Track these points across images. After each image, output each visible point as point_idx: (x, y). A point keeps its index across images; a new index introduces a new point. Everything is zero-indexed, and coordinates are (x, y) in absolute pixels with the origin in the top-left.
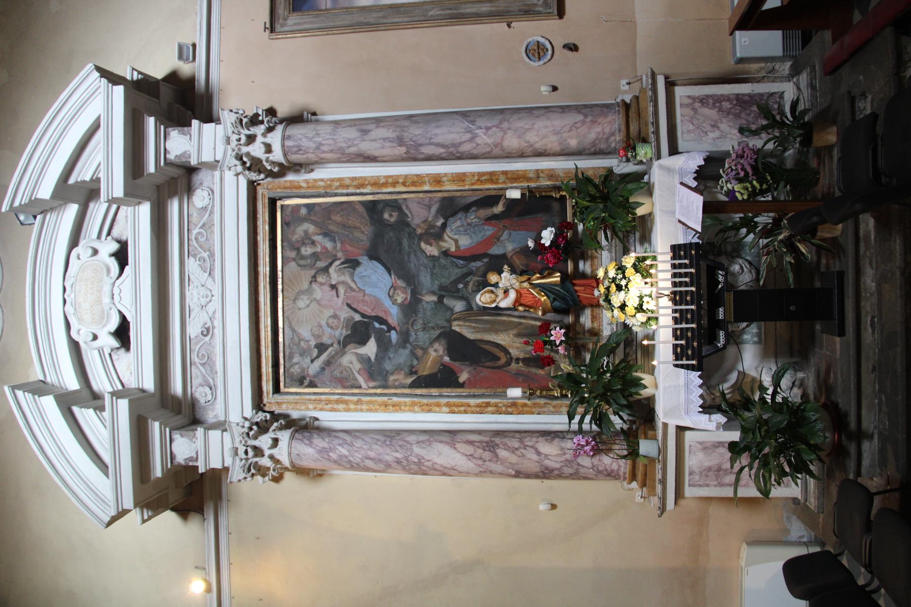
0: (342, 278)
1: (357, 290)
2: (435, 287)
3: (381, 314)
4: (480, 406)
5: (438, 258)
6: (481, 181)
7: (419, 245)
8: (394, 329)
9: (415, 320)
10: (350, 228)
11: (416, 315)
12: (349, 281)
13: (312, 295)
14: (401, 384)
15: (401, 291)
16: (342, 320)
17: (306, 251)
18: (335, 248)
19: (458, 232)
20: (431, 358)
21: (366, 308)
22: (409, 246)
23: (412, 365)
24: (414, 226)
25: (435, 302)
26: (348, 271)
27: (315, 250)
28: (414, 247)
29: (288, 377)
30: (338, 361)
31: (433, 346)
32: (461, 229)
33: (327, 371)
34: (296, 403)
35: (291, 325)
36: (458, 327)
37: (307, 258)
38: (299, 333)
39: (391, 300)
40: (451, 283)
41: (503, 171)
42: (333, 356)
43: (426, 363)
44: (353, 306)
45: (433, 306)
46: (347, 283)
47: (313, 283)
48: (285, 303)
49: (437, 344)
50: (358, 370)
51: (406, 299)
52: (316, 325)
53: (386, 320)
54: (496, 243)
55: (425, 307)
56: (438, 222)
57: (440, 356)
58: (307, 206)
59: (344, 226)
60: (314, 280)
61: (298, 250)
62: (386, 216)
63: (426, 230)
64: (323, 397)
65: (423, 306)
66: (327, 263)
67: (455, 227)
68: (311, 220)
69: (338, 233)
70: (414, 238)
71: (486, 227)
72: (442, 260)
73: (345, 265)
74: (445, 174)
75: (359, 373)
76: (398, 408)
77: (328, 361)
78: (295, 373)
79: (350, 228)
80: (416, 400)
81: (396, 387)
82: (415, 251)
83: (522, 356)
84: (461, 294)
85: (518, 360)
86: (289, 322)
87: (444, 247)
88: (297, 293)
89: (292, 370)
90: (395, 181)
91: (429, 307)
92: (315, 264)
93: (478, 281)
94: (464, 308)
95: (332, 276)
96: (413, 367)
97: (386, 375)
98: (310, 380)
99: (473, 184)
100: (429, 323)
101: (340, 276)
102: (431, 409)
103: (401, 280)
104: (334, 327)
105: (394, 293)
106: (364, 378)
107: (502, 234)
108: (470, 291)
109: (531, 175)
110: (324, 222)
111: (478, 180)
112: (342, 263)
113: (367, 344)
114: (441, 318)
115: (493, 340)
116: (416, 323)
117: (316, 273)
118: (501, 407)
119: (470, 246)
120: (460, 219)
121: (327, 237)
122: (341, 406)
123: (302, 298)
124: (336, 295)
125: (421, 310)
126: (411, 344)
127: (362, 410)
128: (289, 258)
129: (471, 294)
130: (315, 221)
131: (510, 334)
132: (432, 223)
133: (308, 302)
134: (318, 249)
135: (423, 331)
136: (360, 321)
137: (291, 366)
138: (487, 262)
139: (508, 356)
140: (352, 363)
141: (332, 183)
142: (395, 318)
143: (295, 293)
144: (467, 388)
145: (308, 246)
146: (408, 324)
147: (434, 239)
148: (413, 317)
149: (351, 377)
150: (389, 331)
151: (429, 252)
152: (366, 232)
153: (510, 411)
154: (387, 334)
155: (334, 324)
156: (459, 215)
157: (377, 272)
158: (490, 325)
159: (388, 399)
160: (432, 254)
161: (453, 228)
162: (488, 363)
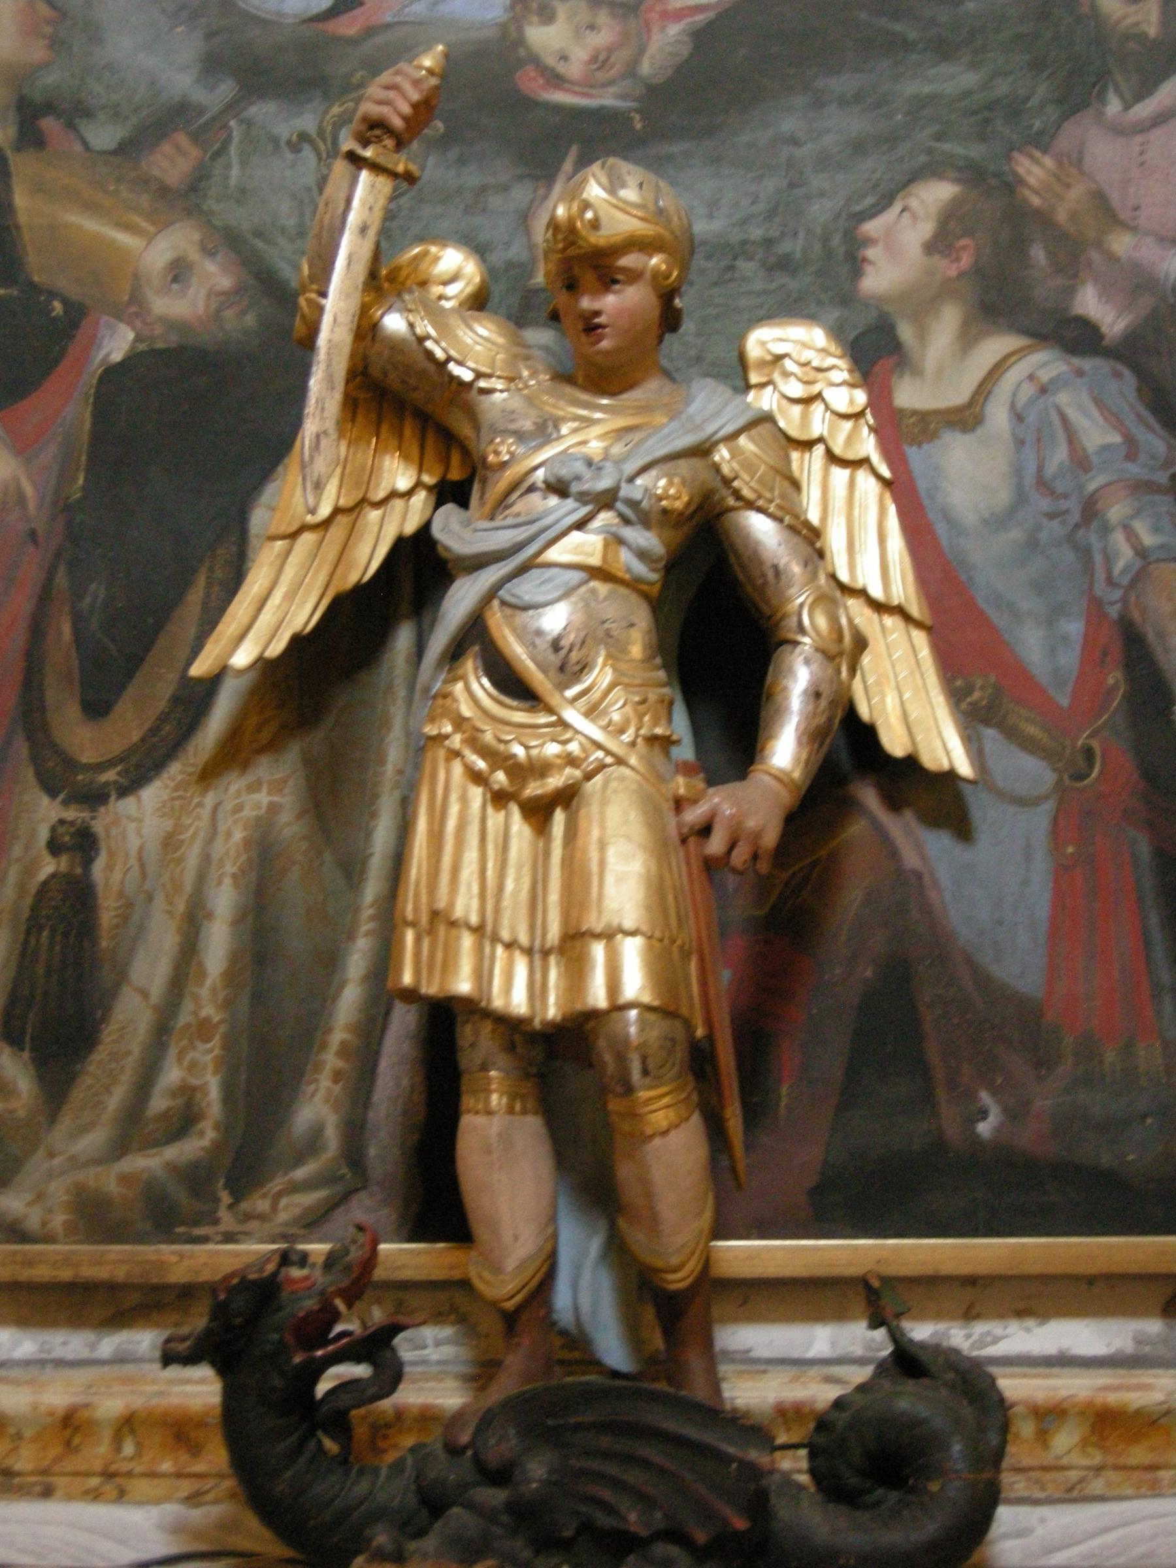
7: (930, 170)
15: (610, 50)
20: (124, 238)
22: (933, 98)
23: (88, 114)
24: (1068, 136)
31: (210, 253)
32: (1059, 455)
43: (90, 207)
51: (557, 80)
55: (495, 201)
56: (1107, 292)
57: (136, 298)
63: (1045, 219)
65: (505, 188)
67: (1073, 414)
70: (983, 138)
71: (1074, 628)
82: (891, 140)
87: (923, 335)
96: (71, 126)
103: (685, 51)
107: (1028, 745)
119: (932, 516)
120: (1131, 449)
125: (472, 178)
126: (231, 107)
132: (1095, 256)
139: (110, 776)
147: (977, 270)
151: (889, 232)
160: (871, 253)
161: (1063, 398)
162: (67, 629)
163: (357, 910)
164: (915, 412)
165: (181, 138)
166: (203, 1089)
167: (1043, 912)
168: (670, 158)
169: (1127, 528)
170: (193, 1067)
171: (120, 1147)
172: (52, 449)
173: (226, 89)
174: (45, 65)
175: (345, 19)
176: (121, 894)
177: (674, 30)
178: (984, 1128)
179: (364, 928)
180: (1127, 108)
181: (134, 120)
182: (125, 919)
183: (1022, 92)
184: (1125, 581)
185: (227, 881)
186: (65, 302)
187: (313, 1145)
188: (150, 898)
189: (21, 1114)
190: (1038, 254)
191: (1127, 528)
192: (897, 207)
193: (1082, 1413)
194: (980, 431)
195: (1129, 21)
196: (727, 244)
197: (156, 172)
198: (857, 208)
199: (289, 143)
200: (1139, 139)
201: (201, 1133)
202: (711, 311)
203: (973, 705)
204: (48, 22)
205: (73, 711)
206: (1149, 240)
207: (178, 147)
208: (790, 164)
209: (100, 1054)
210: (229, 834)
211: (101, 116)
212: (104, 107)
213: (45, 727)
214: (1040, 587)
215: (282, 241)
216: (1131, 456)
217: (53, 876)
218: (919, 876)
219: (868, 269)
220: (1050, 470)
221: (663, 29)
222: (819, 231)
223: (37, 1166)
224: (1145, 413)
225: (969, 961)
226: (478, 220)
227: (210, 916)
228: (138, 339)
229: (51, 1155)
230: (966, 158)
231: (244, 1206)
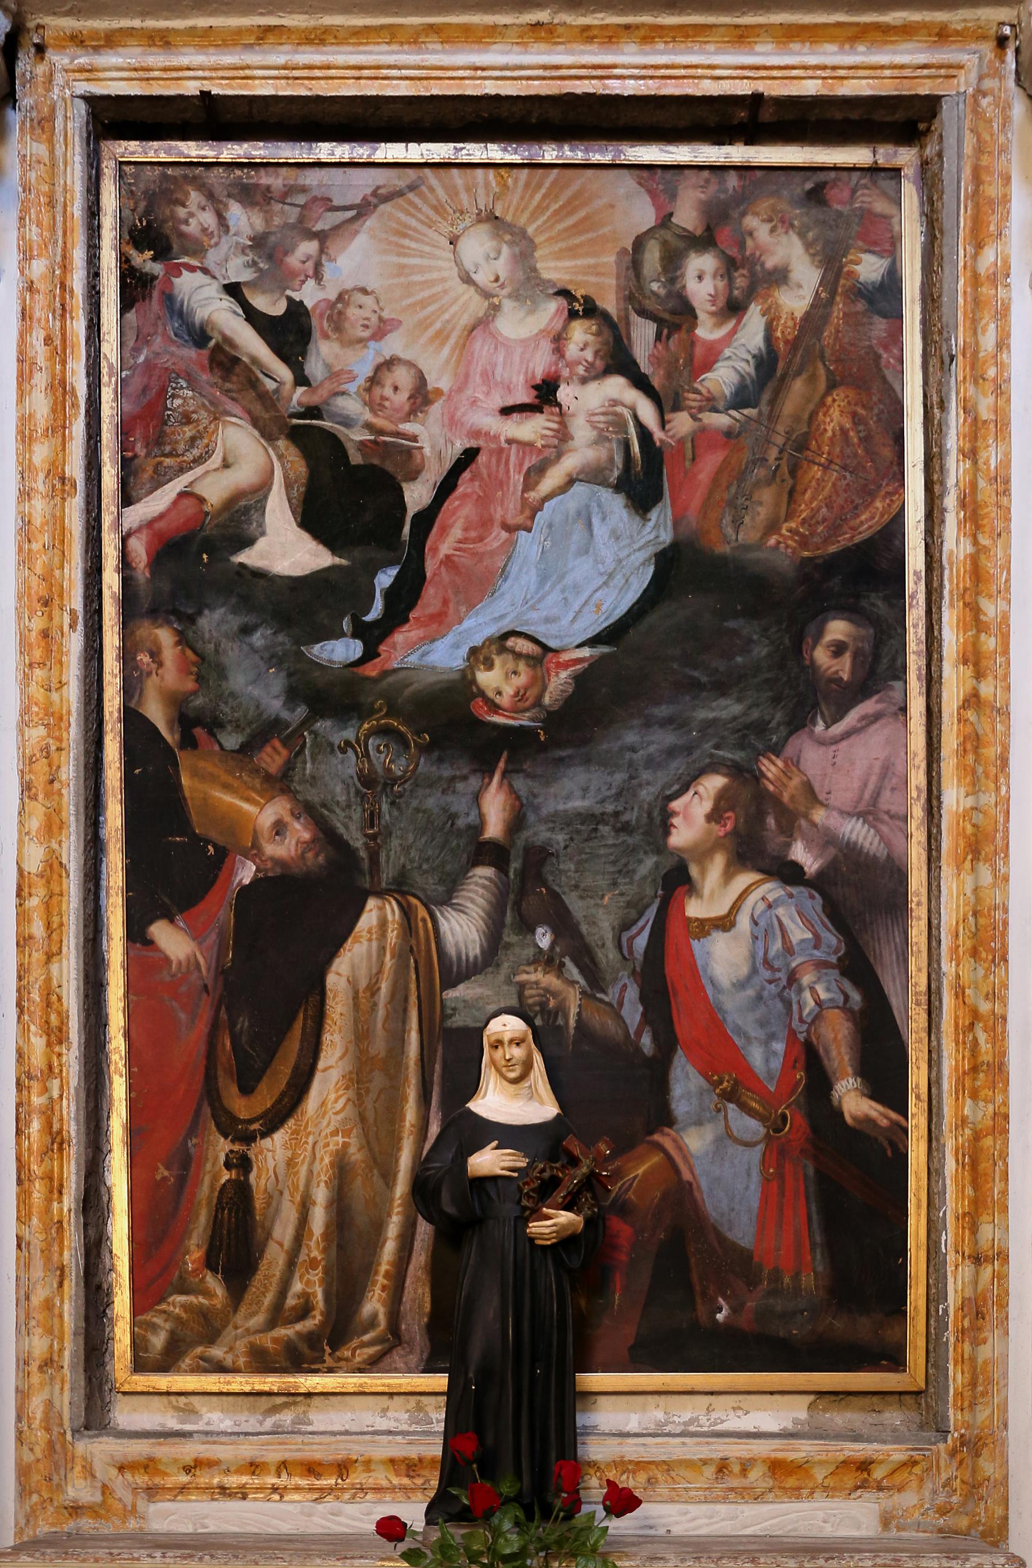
0: (582, 432)
1: (533, 496)
2: (539, 833)
3: (430, 598)
4: (48, 1005)
5: (660, 848)
6: (972, 1024)
8: (370, 654)
9: (406, 745)
10: (793, 472)
11: (425, 749)
12: (570, 463)
13: (515, 296)
14: (140, 680)
16: (407, 427)
17: (700, 278)
18: (711, 404)
19: (761, 932)
20: (246, 806)
21: (456, 532)
22: (714, 722)
23: (221, 726)
24: (789, 750)
25: (479, 827)
26: (611, 460)
27: (702, 316)
28: (707, 746)
29: (165, 177)
30: (230, 406)
31: (297, 818)
32: (777, 946)
33: (191, 353)
34: (51, 204)
35: (387, 198)
36: (374, 922)
37: (672, 281)
38: (357, 232)
39: (490, 640)
40: (556, 897)
41: (1006, 1117)
42: (253, 383)
43: (227, 787)
44: (466, 475)
45: (461, 823)
46: (559, 456)
47: (562, 302)
48: (479, 172)
49: (306, 836)
50: (198, 490)
52: (385, 315)
53: (406, 620)
54: (716, 1084)
55: (460, 786)
56: (808, 847)
57: (256, 845)
58: (891, 284)
59: (802, 445)
60: (577, 306)
61: (705, 241)
62: (838, 629)
63: (776, 800)
64: (79, 326)
65: (465, 778)
66: (645, 367)
67: (786, 921)
68: (831, 302)
69: (773, 417)
70: (741, 746)
71: (779, 1047)
72: (650, 862)
73: (636, 448)
74: (1006, 879)
75: (182, 495)
76: (38, 654)
77: (236, 360)
78: (181, 212)
79: (793, 472)
80: (74, 732)
81: (127, 655)
83: (259, 1181)
84: (509, 937)
85: (242, 1164)
86: (400, 194)
87: (703, 872)
88: (523, 233)
89: (195, 197)
90: (984, 663)
91: (459, 804)
92: (643, 313)
93: (562, 1009)
94: (451, 950)
95: (593, 386)
96: (212, 734)
97: (175, 612)
98: (154, 278)
99: (960, 993)
100: (393, 803)
101: (593, 425)
102: (34, 798)
104: (377, 391)
105: (518, 656)
106: (161, 516)
108: (524, 977)
109: (986, 1231)
110: (822, 358)
111: (975, 1015)
112: (644, 434)
113: (306, 536)
114: (413, 853)
115: (321, 1065)
116: (393, 746)
117: (605, 316)
118: (46, 1090)
121: (758, 367)
122: (41, 405)
123: (499, 253)
124: (510, 402)
125: (447, 772)
126: (306, 723)
127: (25, 494)
128: (673, 196)
129: (509, 981)
130: (825, 319)
131: (347, 1133)
132: (803, 822)
133: (482, 278)
134: (706, 331)
135: (361, 776)
136: (404, 508)
137: (211, 196)
138: (638, 1049)
139: (256, 1126)
140: (226, 465)
141: (989, 387)
142: (413, 659)
143: (522, 221)
144: (127, 953)
145: (721, 284)
146: (387, 715)
147: (735, 833)
148: (418, 733)
149: (168, 461)
150: (361, 631)
151: (686, 806)
152: (772, 541)
153: (28, 1124)
154: (346, 624)
155: (388, 391)
156: (831, 938)
157: (605, 584)
158: (383, 1054)
159: (73, 612)
160: (675, 821)
161: (780, 911)
162: (228, 1044)
163: (392, 1200)
164: (697, 919)
165: (277, 743)
166: (315, 1295)
167: (755, 1204)
168: (561, 759)
169: (812, 989)
170: (308, 1283)
171: (272, 1323)
172: (213, 936)
173: (301, 711)
174: (195, 693)
175: (369, 665)
176: (266, 1189)
177: (564, 675)
178: (720, 1317)
179: (396, 1210)
180: (827, 727)
181: (248, 731)
182: (268, 1204)
183: (767, 718)
184: (809, 1020)
185: (322, 1184)
186: (215, 846)
187: (372, 1323)
188: (281, 1193)
189: (219, 1306)
190: (771, 821)
191: (812, 989)
192: (691, 792)
193: (764, 1461)
194: (733, 932)
195: (833, 669)
196: (593, 815)
197: (264, 765)
198: (668, 793)
199: (339, 747)
200: (834, 748)
201: (314, 1317)
202: (584, 856)
203: (724, 1090)
204: (194, 664)
205: (234, 1089)
206: (835, 814)
207: (274, 748)
208: (631, 764)
209: (259, 1276)
210: (322, 1159)
211: (229, 728)
212: (230, 722)
213: (219, 1098)
214: (762, 1023)
215: (338, 810)
216: (816, 947)
217: (228, 1181)
218: (690, 1184)
219: (674, 831)
220: (772, 953)
221: (557, 674)
222: (646, 806)
223: (229, 1333)
224: (826, 920)
225: (715, 1229)
226: (450, 798)
227: (314, 1203)
228: (258, 870)
229: (236, 1328)
230: (732, 760)
231: (338, 1353)
